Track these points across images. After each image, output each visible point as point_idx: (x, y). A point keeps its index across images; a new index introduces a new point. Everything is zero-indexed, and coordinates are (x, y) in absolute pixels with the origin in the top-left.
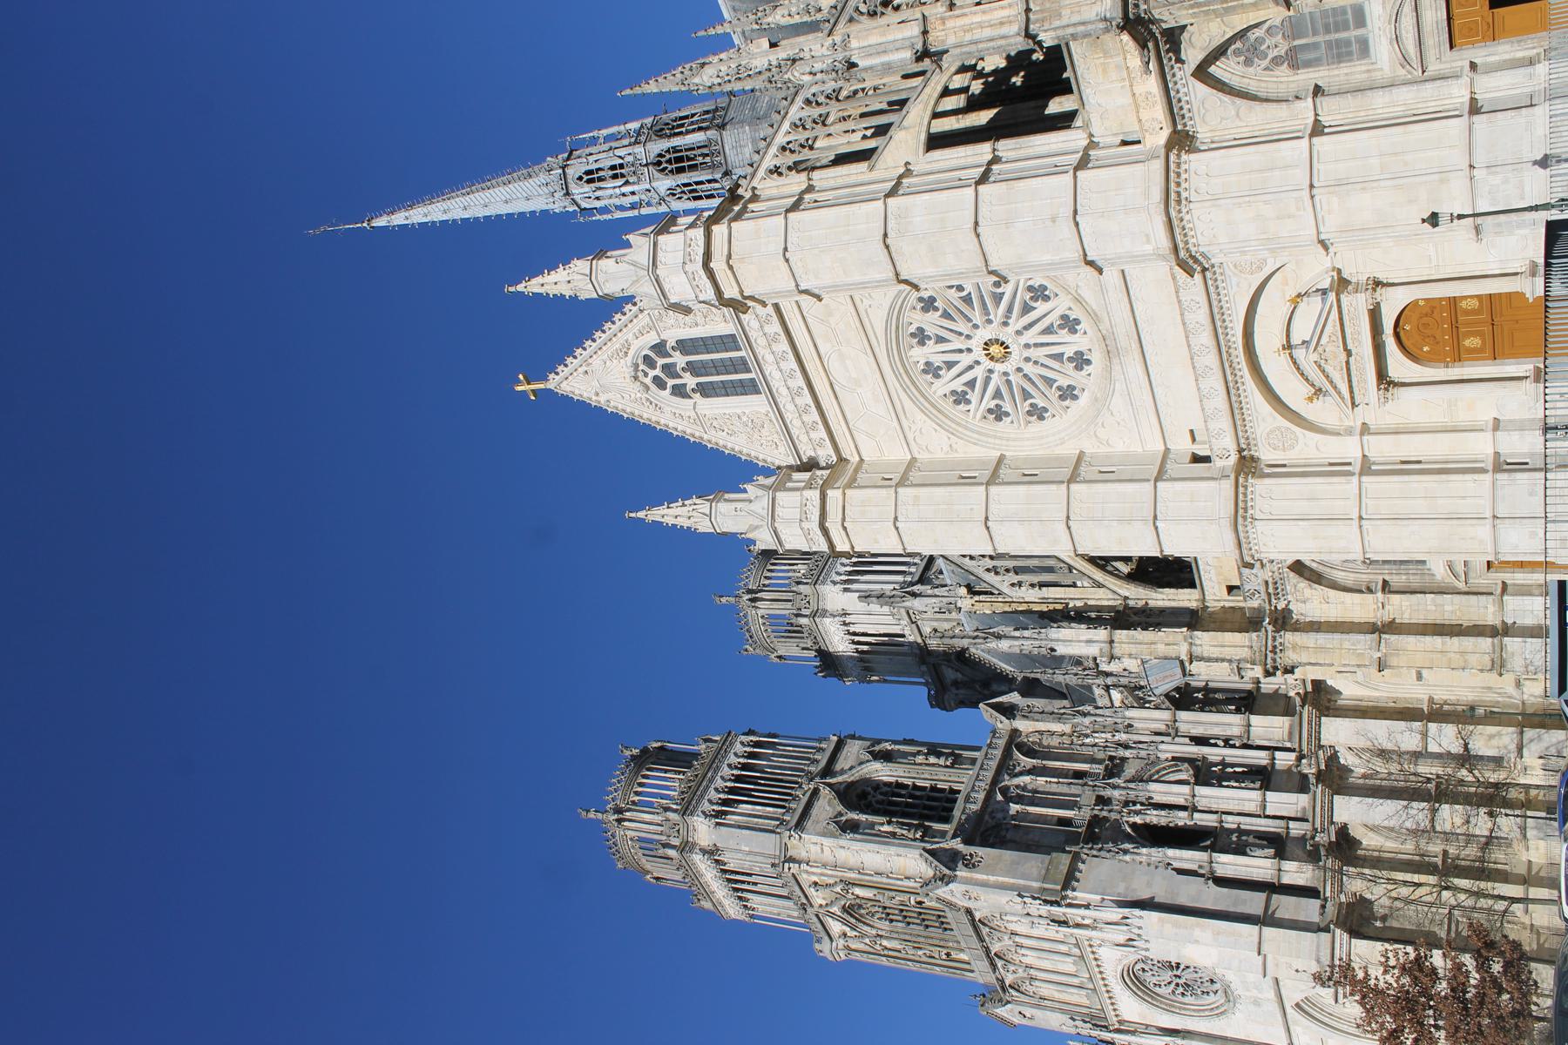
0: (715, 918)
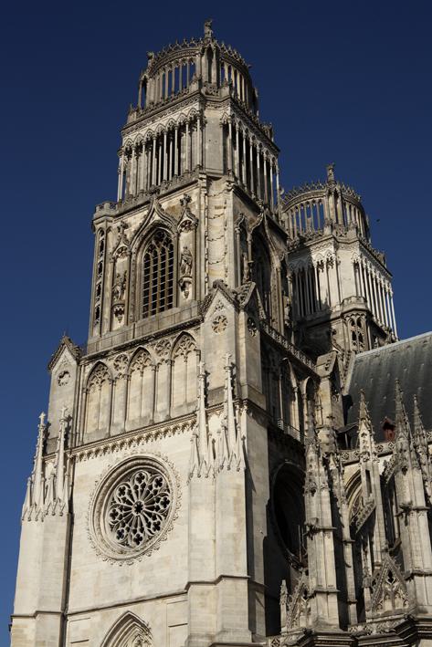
0: (121, 127)
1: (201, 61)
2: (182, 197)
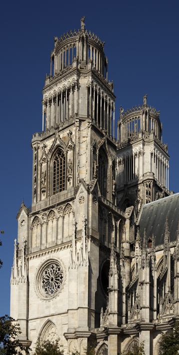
0: (42, 88)
2: (68, 132)
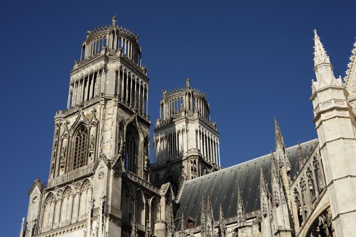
0: (70, 71)
1: (109, 38)
2: (92, 109)
